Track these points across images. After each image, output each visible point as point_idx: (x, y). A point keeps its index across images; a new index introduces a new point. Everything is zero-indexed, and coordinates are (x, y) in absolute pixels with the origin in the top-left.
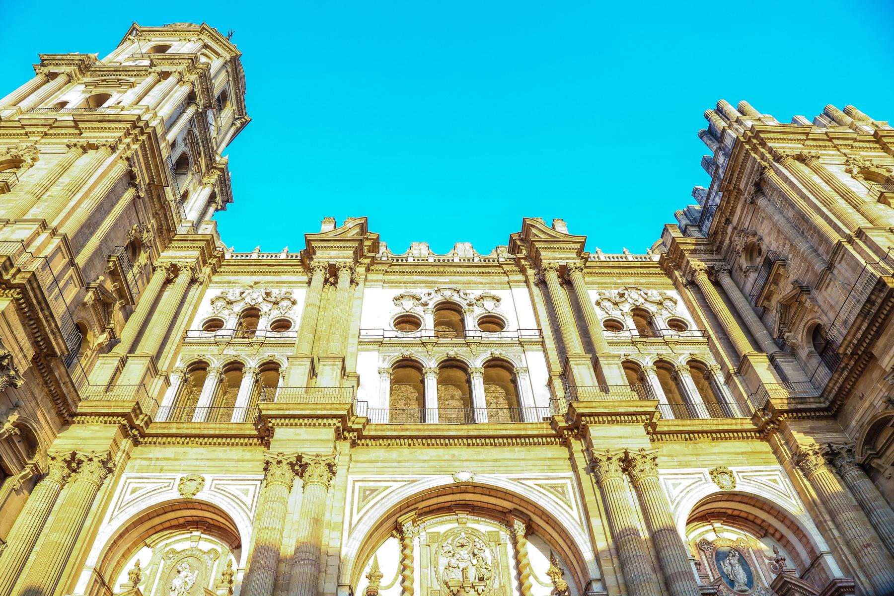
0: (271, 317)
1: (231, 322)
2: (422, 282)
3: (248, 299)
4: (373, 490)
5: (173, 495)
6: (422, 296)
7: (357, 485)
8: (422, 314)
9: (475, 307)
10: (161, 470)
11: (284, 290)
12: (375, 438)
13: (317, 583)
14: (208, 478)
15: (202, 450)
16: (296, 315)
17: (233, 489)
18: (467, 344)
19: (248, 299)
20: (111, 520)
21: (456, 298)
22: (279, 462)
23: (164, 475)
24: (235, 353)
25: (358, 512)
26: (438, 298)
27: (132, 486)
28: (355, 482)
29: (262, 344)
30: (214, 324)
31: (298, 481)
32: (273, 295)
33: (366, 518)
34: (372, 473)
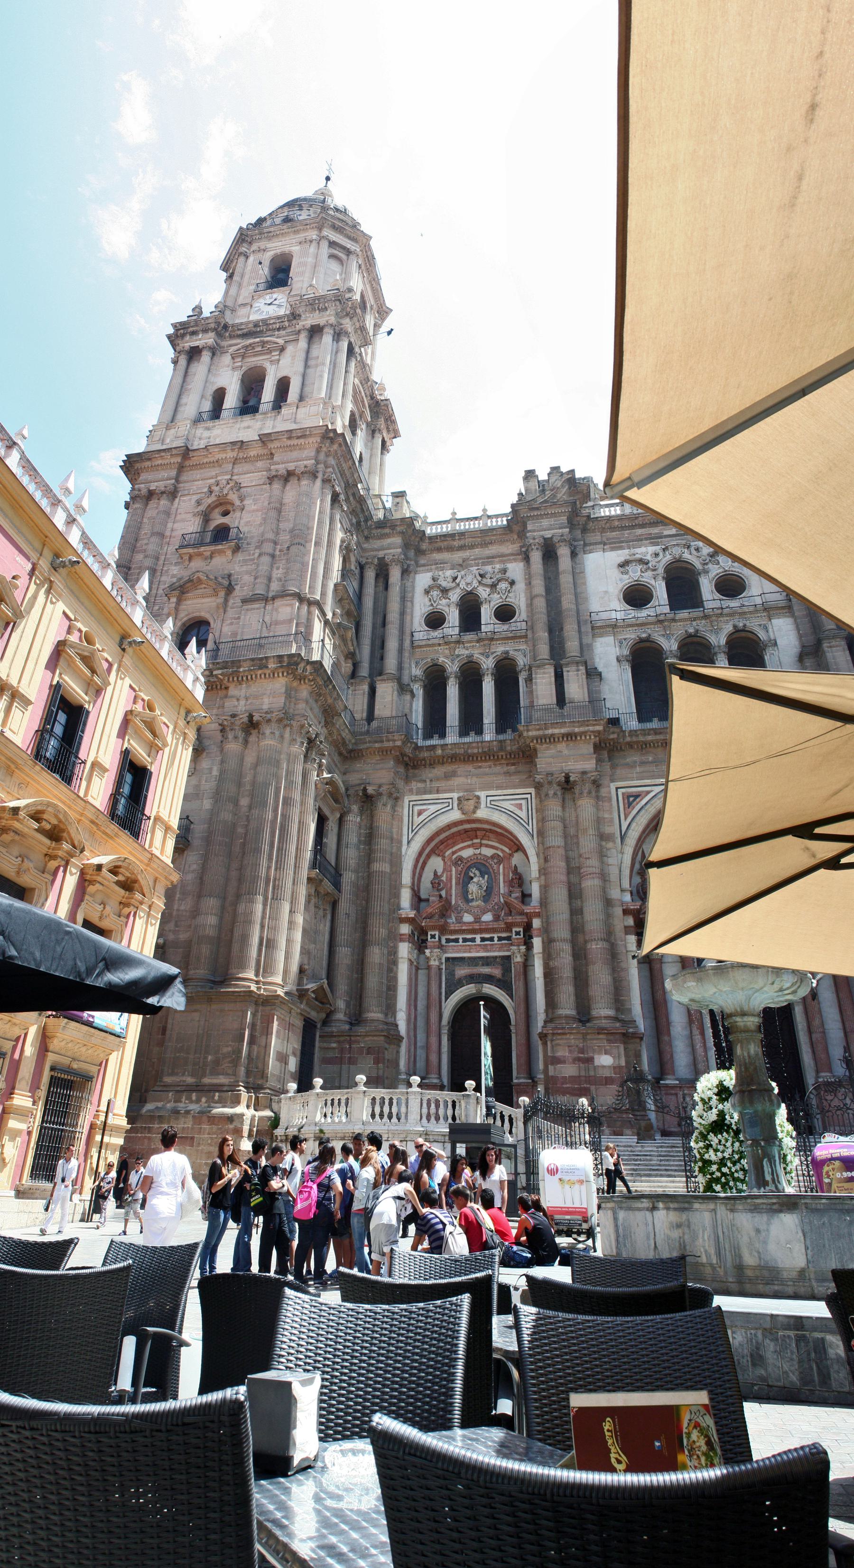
0: (492, 604)
1: (453, 617)
2: (646, 539)
3: (463, 585)
4: (637, 796)
5: (456, 815)
6: (648, 557)
7: (620, 791)
8: (652, 582)
9: (710, 566)
10: (438, 792)
11: (498, 566)
12: (630, 745)
13: (604, 892)
14: (482, 794)
15: (469, 768)
16: (519, 599)
17: (507, 805)
18: (706, 617)
19: (463, 585)
20: (409, 842)
21: (686, 556)
22: (550, 783)
23: (441, 796)
24: (467, 652)
25: (626, 819)
26: (667, 558)
27: (416, 808)
28: (617, 789)
29: (492, 639)
30: (435, 621)
31: (568, 796)
32: (488, 576)
33: (634, 825)
34: (632, 779)
